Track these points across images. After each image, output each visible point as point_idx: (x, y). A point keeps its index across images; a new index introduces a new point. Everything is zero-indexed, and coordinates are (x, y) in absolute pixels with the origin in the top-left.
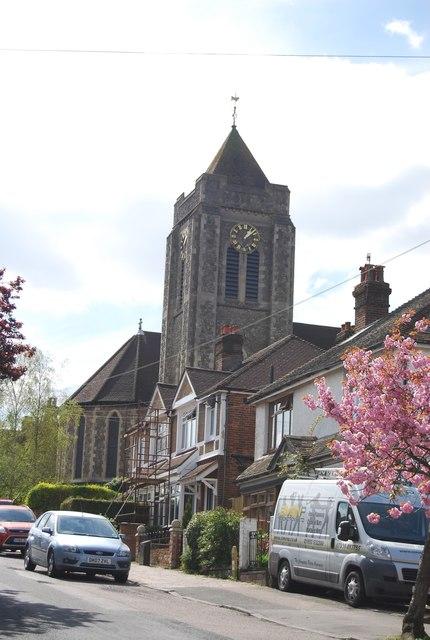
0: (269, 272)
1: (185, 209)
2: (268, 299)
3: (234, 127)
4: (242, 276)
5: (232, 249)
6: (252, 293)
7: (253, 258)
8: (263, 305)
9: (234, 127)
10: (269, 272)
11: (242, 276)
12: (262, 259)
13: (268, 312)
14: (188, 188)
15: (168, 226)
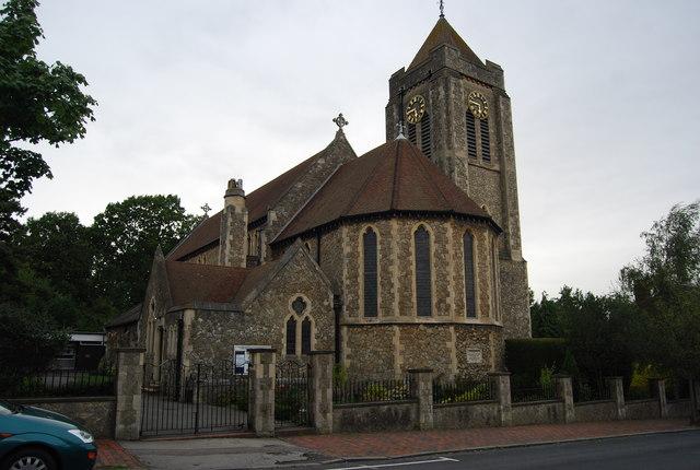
0: (499, 142)
1: (400, 84)
2: (500, 160)
3: (442, 16)
4: (478, 134)
5: (470, 115)
6: (486, 158)
7: (484, 122)
8: (497, 167)
9: (442, 16)
10: (499, 142)
11: (478, 134)
12: (491, 123)
13: (501, 173)
14: (405, 60)
15: (384, 96)
